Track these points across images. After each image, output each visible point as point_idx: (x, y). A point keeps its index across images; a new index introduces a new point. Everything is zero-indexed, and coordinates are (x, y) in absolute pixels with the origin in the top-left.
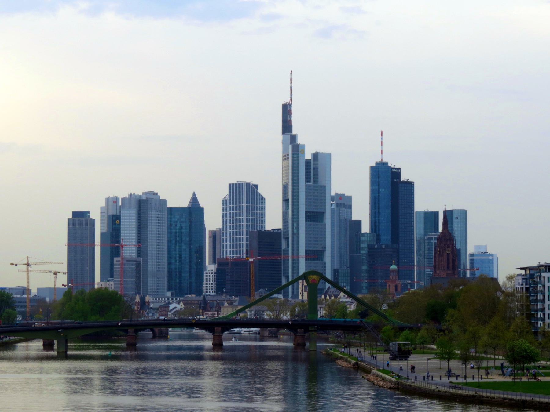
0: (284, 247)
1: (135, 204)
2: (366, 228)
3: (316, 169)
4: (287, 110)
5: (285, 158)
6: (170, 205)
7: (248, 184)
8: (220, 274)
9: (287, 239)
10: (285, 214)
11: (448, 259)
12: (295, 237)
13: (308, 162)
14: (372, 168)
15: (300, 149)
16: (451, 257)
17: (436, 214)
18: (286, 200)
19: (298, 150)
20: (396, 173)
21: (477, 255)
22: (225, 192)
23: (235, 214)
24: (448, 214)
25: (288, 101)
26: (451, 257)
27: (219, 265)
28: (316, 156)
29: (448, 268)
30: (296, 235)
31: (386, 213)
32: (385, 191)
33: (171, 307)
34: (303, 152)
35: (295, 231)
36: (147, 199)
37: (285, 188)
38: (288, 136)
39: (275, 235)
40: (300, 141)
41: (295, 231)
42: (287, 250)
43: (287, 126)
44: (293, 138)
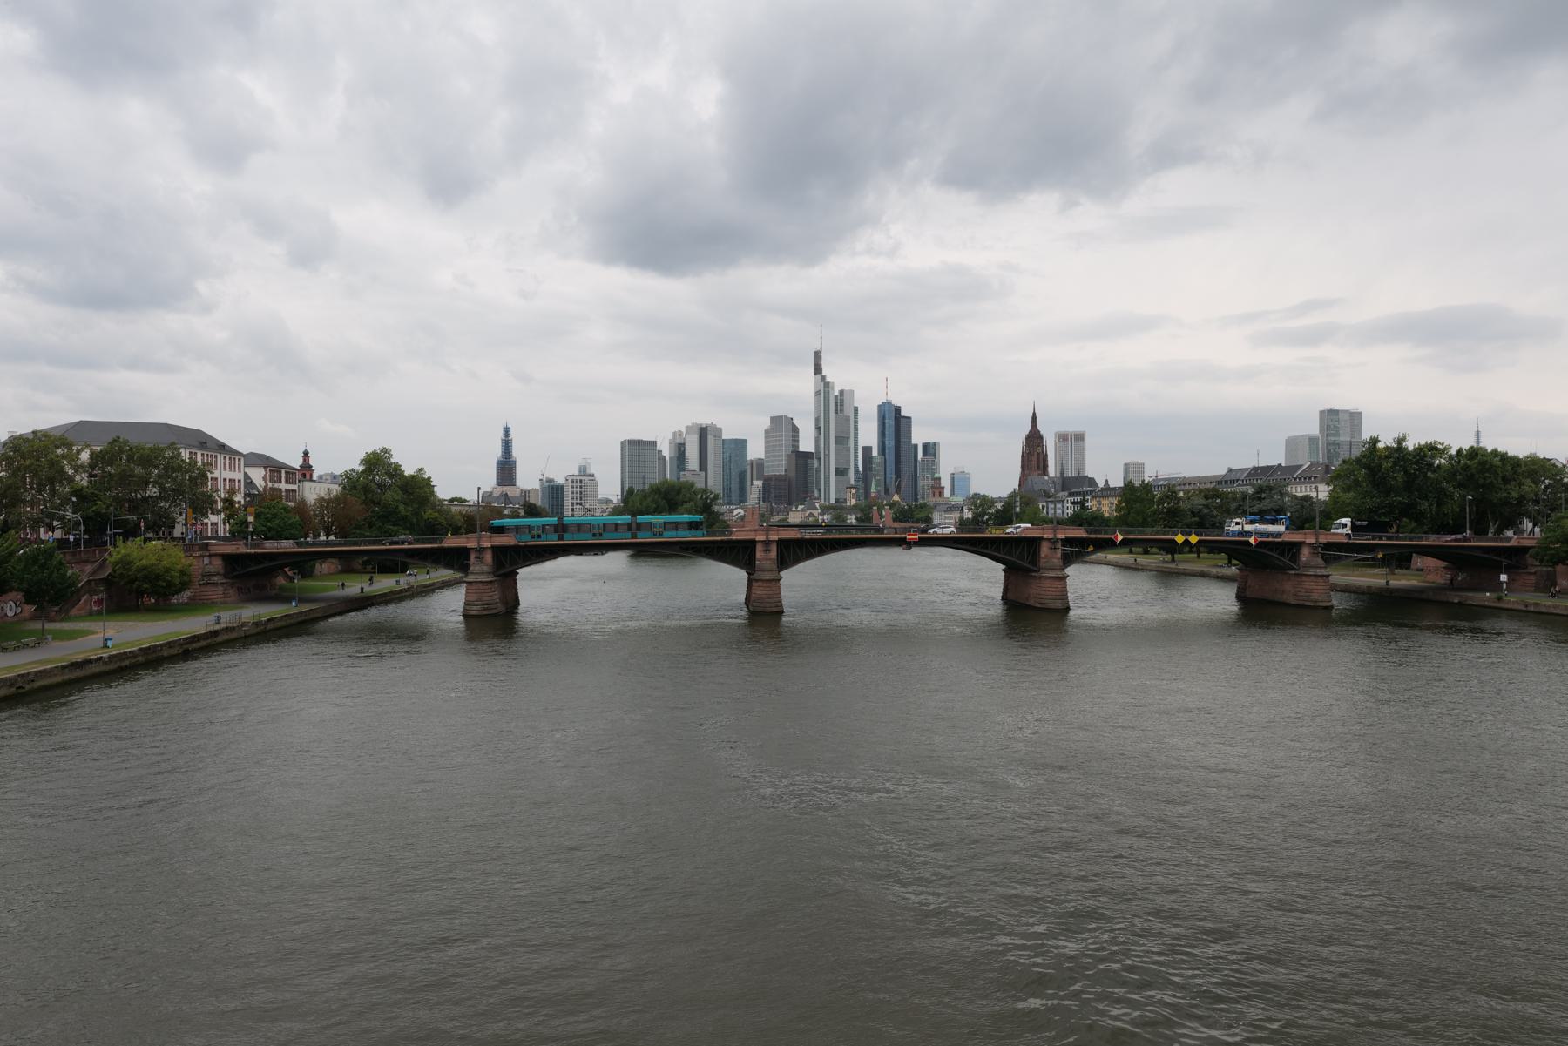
0: (816, 465)
1: (697, 431)
2: (875, 453)
3: (842, 401)
4: (817, 356)
5: (818, 393)
6: (724, 437)
7: (786, 417)
8: (766, 491)
9: (820, 459)
10: (817, 441)
11: (1038, 459)
12: (827, 457)
13: (836, 397)
14: (879, 406)
15: (831, 385)
16: (1041, 457)
17: (916, 446)
18: (818, 428)
19: (828, 387)
20: (898, 410)
21: (958, 474)
22: (767, 424)
23: (776, 441)
24: (926, 447)
25: (818, 349)
26: (1041, 457)
27: (765, 480)
28: (842, 392)
29: (1039, 467)
30: (827, 456)
31: (890, 443)
32: (890, 422)
33: (735, 512)
34: (833, 388)
35: (827, 452)
36: (706, 427)
37: (817, 420)
38: (819, 376)
39: (808, 455)
40: (828, 380)
41: (827, 452)
42: (818, 470)
43: (818, 369)
44: (823, 378)
